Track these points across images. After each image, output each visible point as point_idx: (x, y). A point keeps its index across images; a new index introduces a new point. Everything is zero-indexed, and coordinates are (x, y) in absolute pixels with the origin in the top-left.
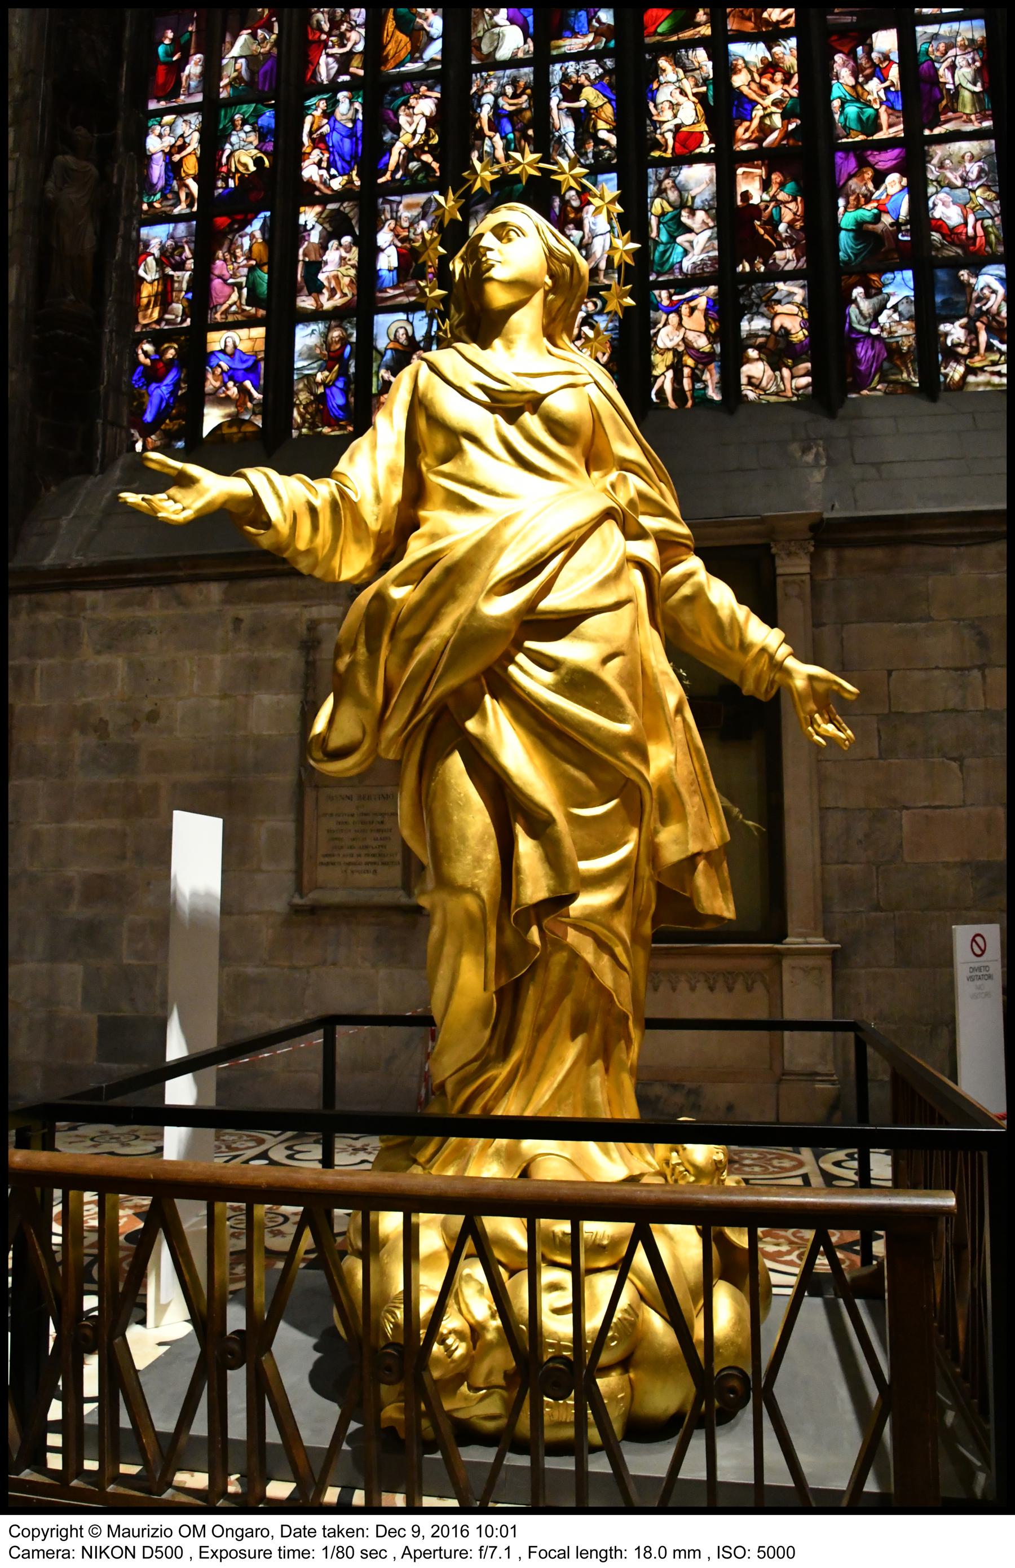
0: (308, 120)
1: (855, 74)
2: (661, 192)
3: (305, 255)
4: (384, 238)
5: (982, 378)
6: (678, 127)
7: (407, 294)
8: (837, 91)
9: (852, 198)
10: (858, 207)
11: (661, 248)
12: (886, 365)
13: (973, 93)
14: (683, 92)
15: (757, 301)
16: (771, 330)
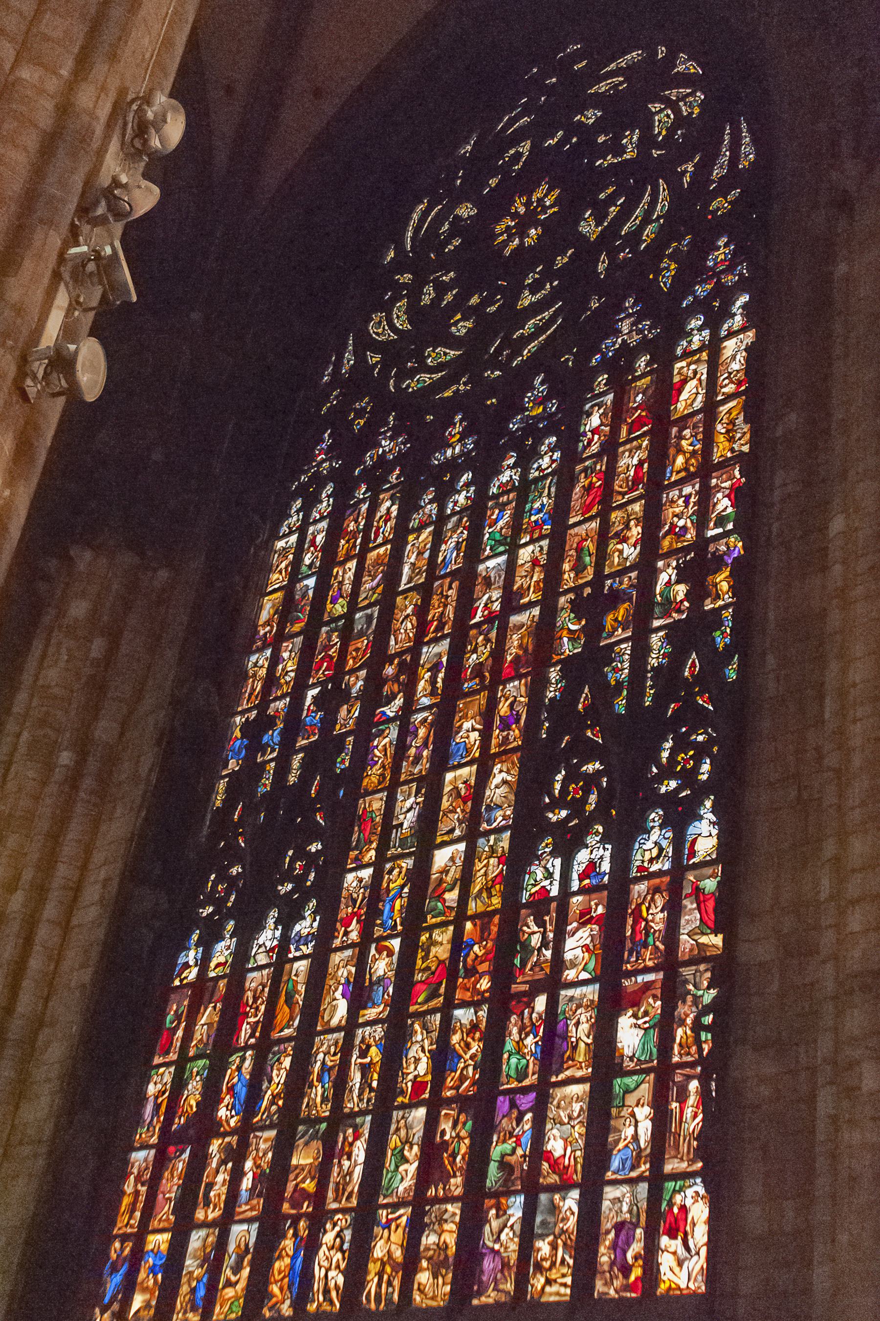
0: (229, 1071)
1: (520, 1033)
2: (398, 1129)
3: (207, 1177)
4: (249, 1164)
5: (554, 1288)
6: (416, 1077)
7: (252, 1209)
8: (509, 1045)
9: (502, 1134)
10: (504, 1141)
11: (389, 1176)
12: (499, 1276)
13: (587, 1044)
14: (423, 1048)
15: (434, 1220)
16: (438, 1245)
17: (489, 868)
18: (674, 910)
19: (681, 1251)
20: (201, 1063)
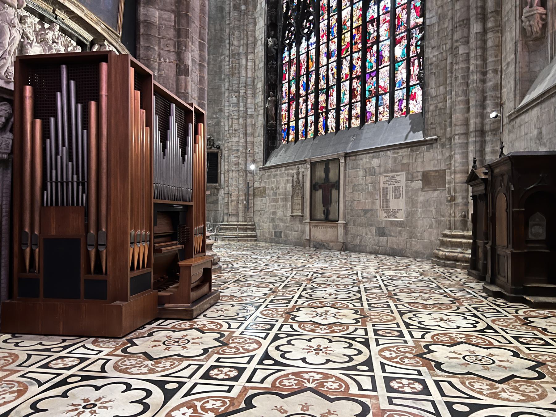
4: (309, 103)
5: (385, 117)
17: (357, 13)
18: (409, 14)
19: (415, 103)
20: (294, 80)
